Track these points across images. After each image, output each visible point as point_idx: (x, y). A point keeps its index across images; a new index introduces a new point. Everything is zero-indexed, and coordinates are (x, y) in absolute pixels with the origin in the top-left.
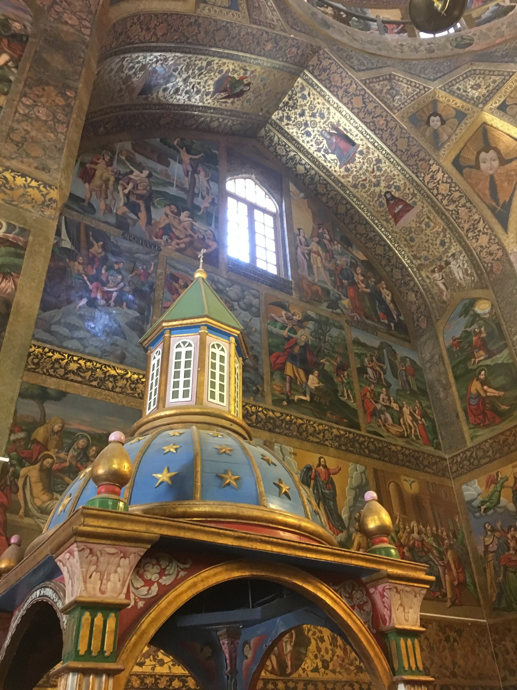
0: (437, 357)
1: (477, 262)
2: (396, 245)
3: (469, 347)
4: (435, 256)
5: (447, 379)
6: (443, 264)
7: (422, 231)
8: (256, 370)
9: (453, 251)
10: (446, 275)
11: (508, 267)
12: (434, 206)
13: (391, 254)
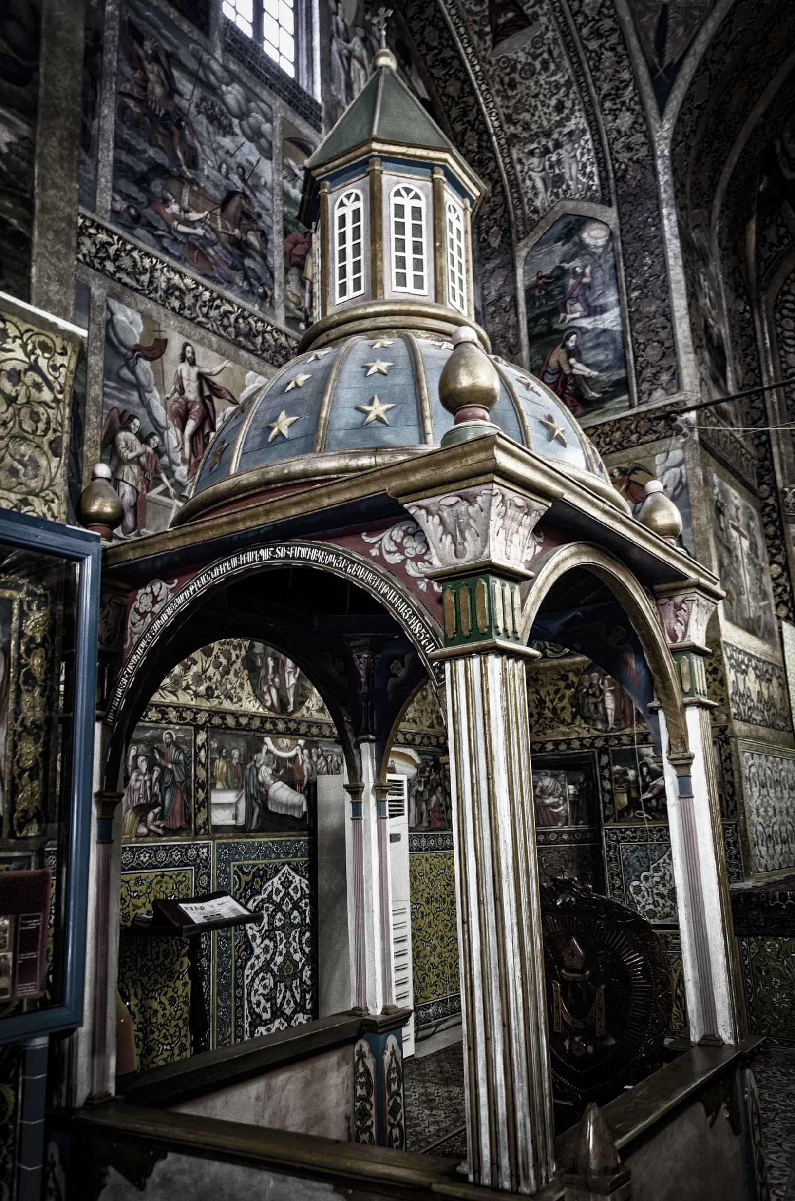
0: (508, 299)
1: (604, 157)
2: (484, 87)
3: (560, 294)
4: (541, 126)
5: (517, 336)
6: (551, 145)
7: (533, 74)
8: (264, 258)
9: (571, 125)
10: (552, 166)
11: (650, 177)
12: (565, 33)
13: (471, 100)
